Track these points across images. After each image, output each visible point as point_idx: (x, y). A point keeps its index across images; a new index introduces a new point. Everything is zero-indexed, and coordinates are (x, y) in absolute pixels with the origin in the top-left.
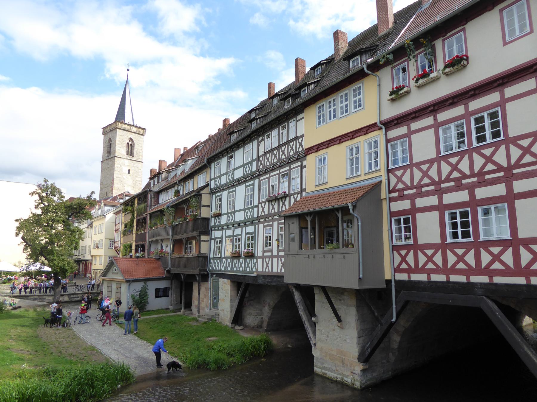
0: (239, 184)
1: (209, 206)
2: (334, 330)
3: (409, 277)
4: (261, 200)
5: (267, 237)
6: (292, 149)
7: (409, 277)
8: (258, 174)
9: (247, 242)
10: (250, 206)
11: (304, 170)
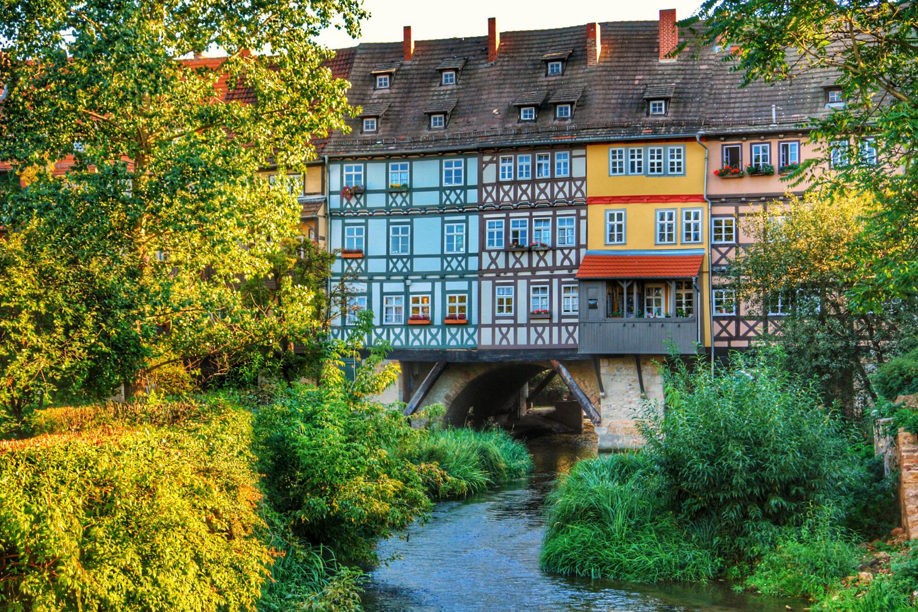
0: (424, 215)
1: (323, 239)
2: (630, 403)
3: (729, 344)
4: (488, 247)
5: (501, 301)
6: (561, 190)
7: (729, 344)
8: (481, 209)
9: (448, 304)
10: (455, 252)
11: (583, 222)
